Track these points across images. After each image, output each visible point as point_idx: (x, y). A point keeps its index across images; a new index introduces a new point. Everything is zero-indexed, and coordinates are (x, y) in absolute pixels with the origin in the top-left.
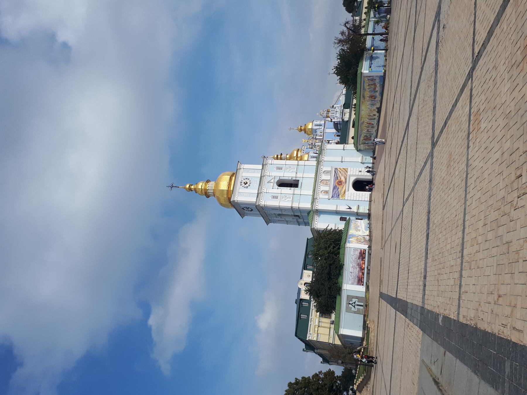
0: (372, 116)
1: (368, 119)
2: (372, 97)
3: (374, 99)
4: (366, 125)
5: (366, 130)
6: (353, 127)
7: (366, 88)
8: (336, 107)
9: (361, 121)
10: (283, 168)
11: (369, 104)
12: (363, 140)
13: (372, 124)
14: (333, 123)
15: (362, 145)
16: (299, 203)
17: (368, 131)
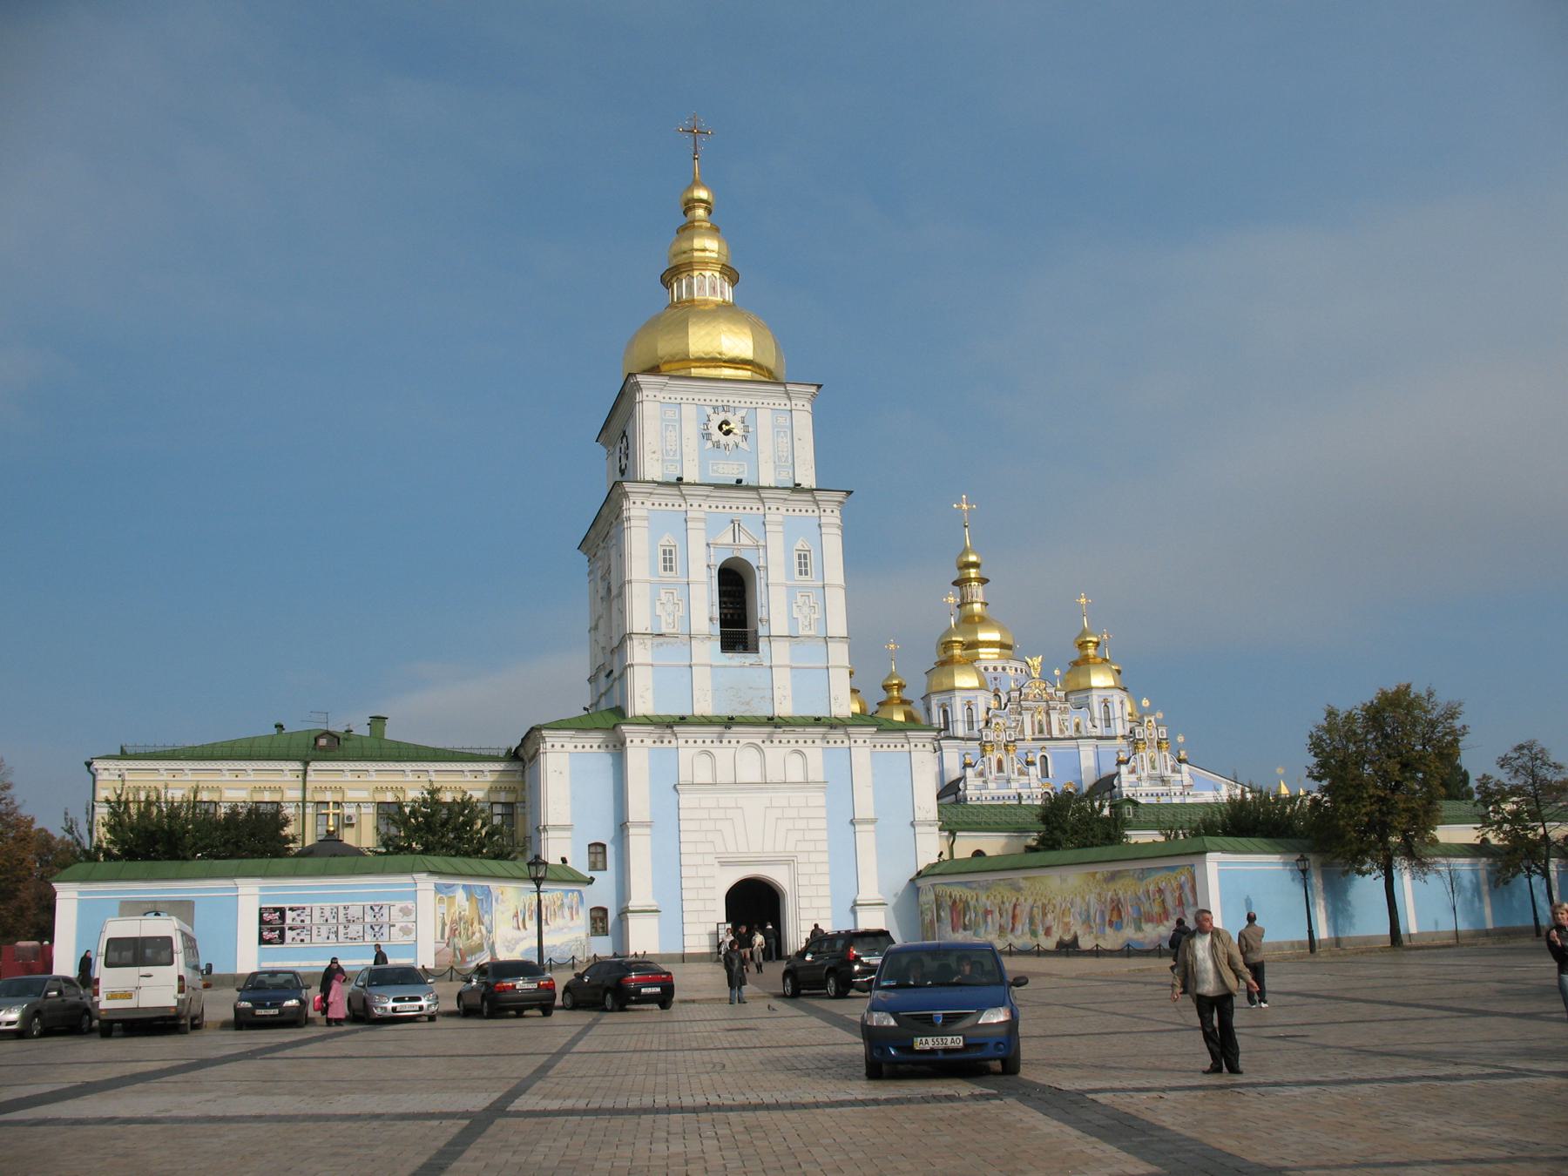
0: (1043, 922)
1: (1032, 908)
2: (1115, 913)
3: (1110, 920)
4: (1010, 903)
5: (988, 903)
6: (1026, 847)
7: (1151, 879)
8: (1180, 772)
9: (1021, 880)
10: (808, 578)
11: (1088, 905)
12: (951, 897)
13: (1013, 924)
14: (1113, 770)
15: (933, 897)
16: (652, 665)
17: (987, 913)
